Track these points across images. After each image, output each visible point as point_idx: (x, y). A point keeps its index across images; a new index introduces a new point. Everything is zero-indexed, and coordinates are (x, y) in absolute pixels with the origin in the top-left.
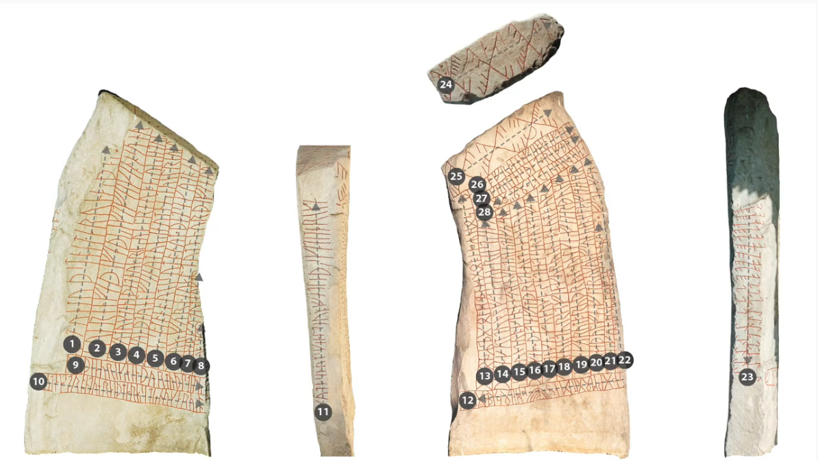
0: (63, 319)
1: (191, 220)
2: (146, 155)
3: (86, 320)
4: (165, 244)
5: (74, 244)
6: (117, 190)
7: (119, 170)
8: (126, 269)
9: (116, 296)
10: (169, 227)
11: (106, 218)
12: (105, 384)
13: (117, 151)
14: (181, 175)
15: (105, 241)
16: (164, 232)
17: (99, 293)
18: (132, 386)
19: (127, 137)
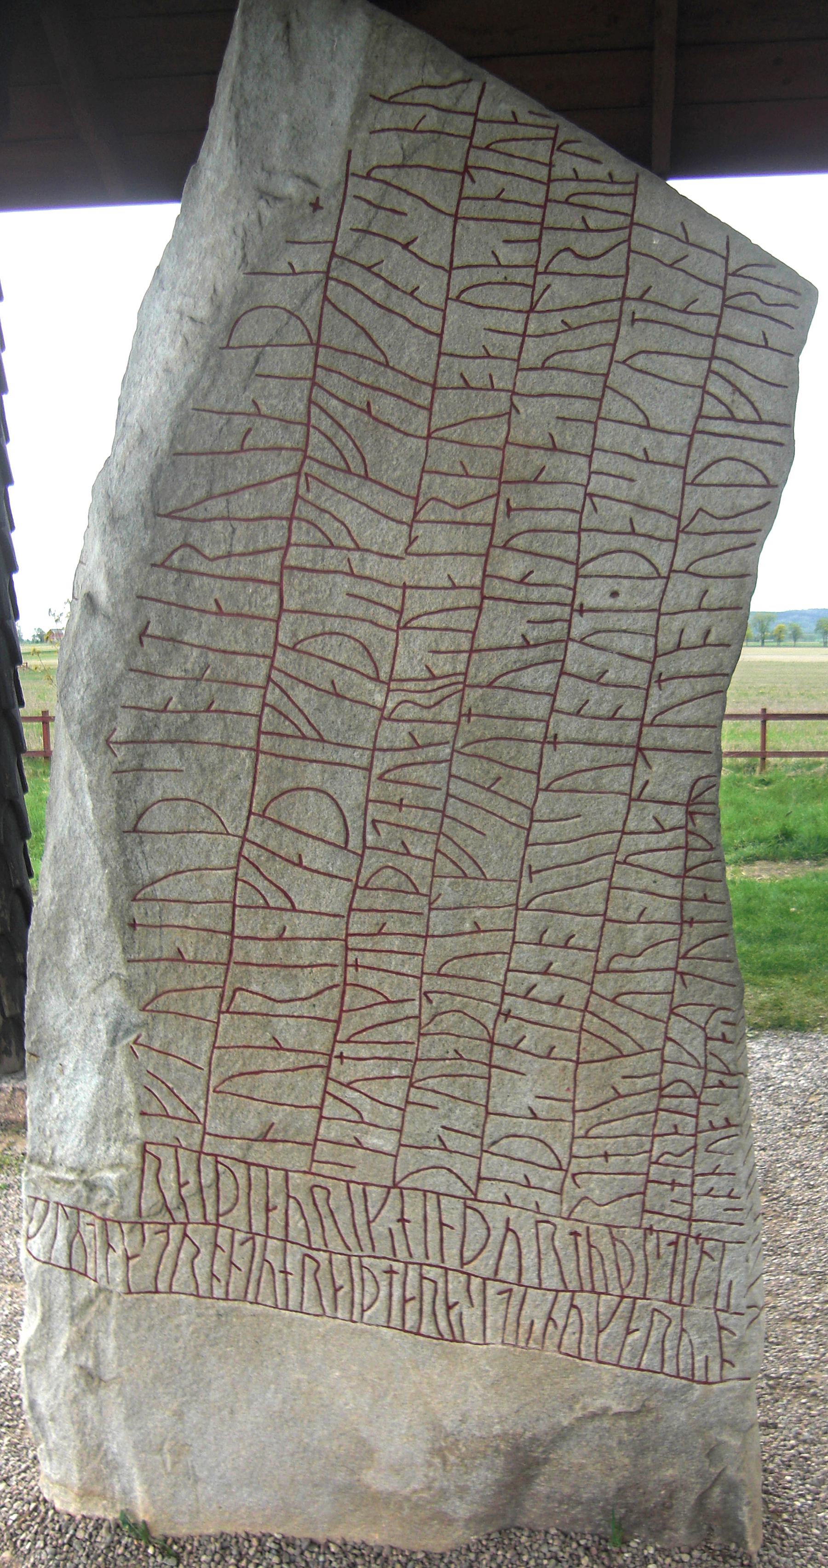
0: (113, 995)
1: (679, 531)
2: (456, 217)
3: (212, 997)
4: (555, 652)
5: (139, 662)
6: (320, 397)
7: (325, 298)
8: (376, 771)
9: (334, 896)
10: (578, 565)
11: (274, 534)
12: (310, 1264)
13: (316, 206)
14: (630, 306)
15: (276, 643)
16: (551, 594)
17: (261, 884)
18: (422, 1277)
19: (362, 135)
